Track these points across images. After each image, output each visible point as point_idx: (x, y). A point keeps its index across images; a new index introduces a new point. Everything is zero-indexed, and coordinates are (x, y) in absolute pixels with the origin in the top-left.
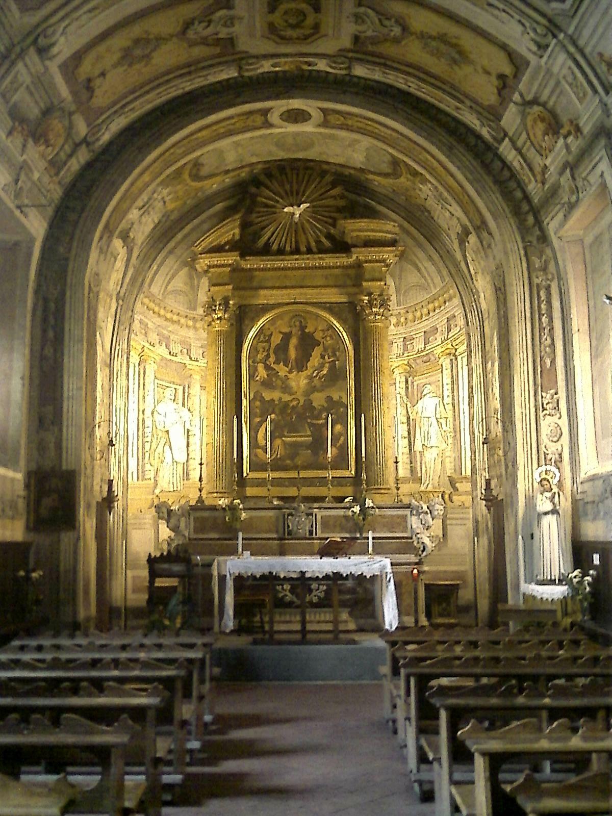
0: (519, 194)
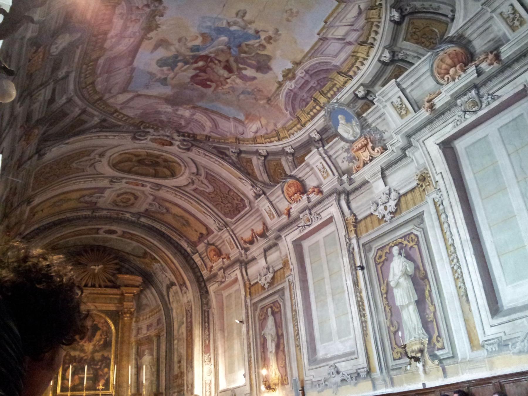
0: (199, 274)
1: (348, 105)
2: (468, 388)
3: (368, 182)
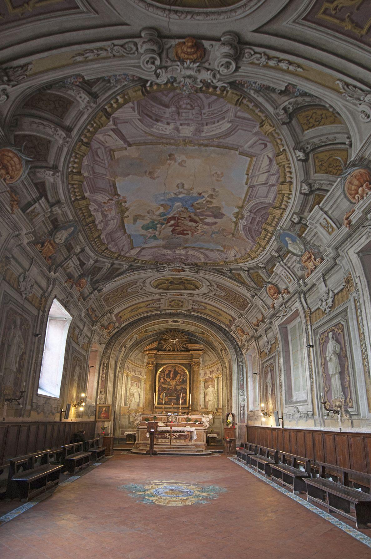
1: (290, 230)
3: (315, 284)
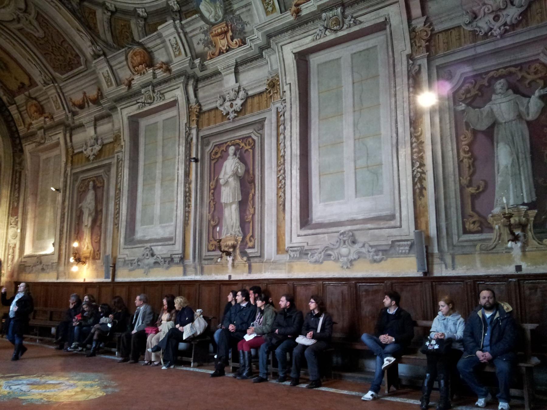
0: (14, 129)
2: (267, 284)
3: (220, 73)
